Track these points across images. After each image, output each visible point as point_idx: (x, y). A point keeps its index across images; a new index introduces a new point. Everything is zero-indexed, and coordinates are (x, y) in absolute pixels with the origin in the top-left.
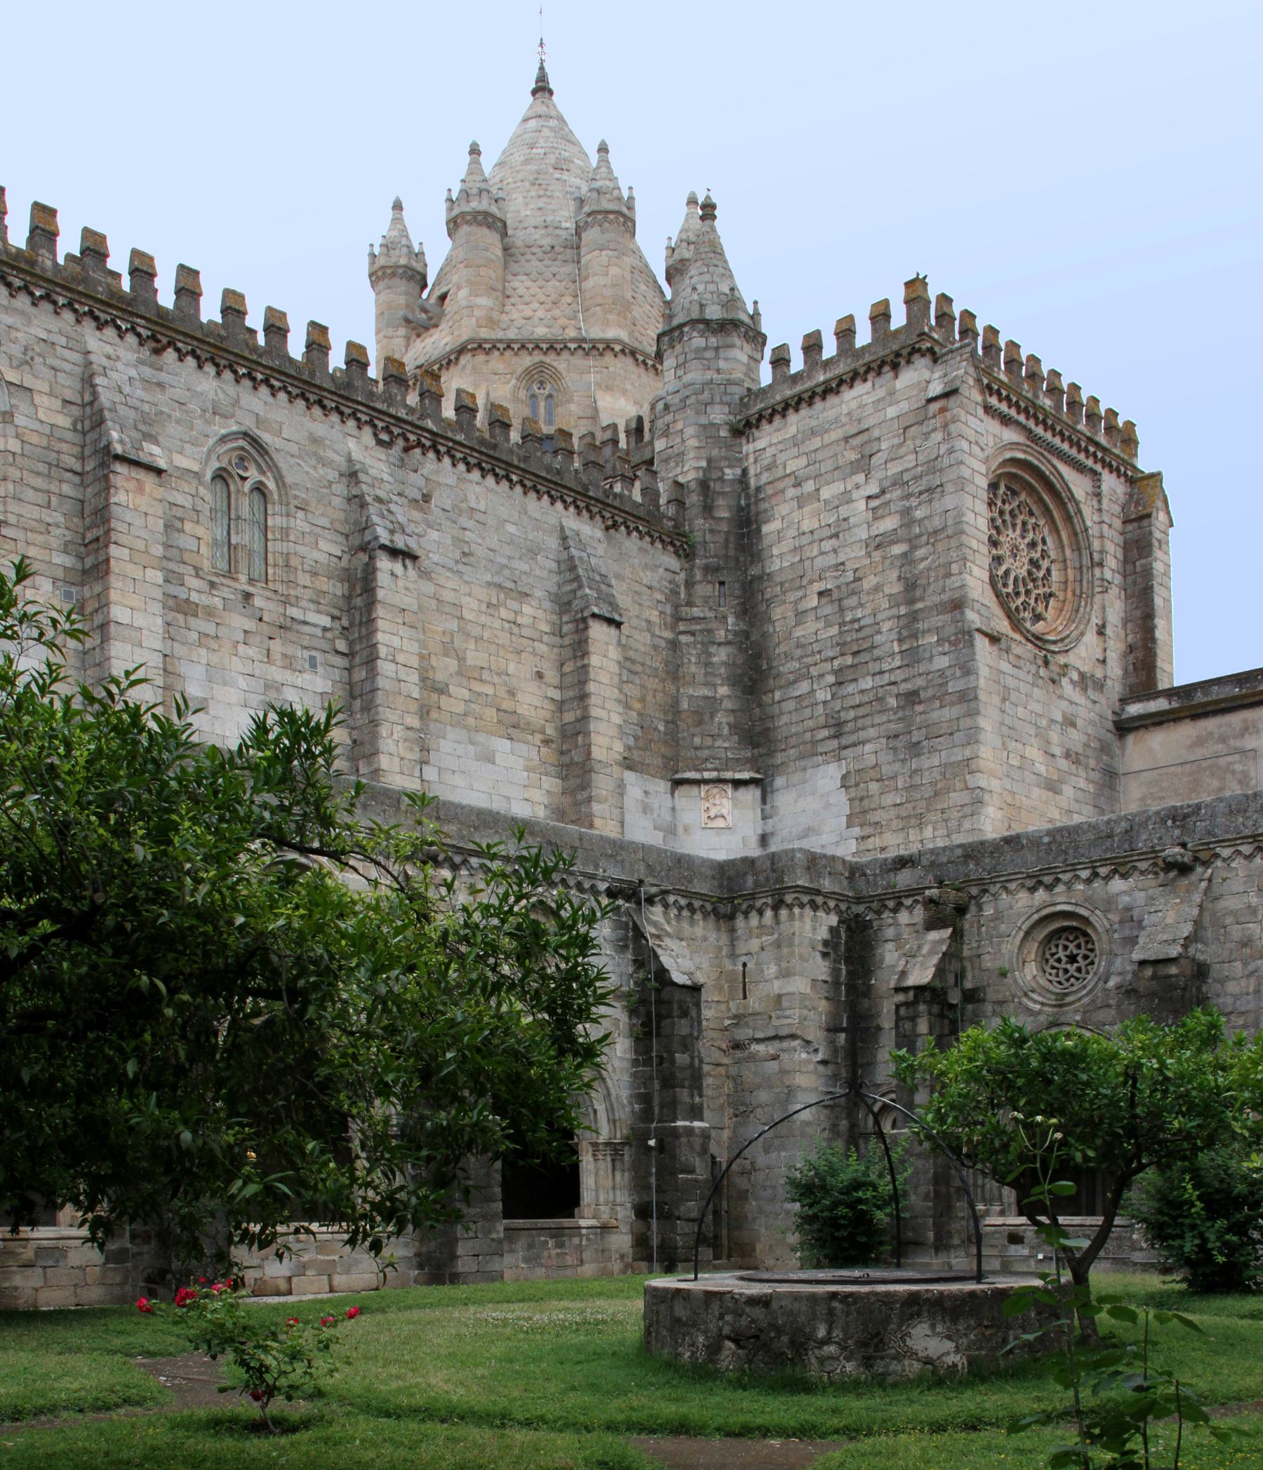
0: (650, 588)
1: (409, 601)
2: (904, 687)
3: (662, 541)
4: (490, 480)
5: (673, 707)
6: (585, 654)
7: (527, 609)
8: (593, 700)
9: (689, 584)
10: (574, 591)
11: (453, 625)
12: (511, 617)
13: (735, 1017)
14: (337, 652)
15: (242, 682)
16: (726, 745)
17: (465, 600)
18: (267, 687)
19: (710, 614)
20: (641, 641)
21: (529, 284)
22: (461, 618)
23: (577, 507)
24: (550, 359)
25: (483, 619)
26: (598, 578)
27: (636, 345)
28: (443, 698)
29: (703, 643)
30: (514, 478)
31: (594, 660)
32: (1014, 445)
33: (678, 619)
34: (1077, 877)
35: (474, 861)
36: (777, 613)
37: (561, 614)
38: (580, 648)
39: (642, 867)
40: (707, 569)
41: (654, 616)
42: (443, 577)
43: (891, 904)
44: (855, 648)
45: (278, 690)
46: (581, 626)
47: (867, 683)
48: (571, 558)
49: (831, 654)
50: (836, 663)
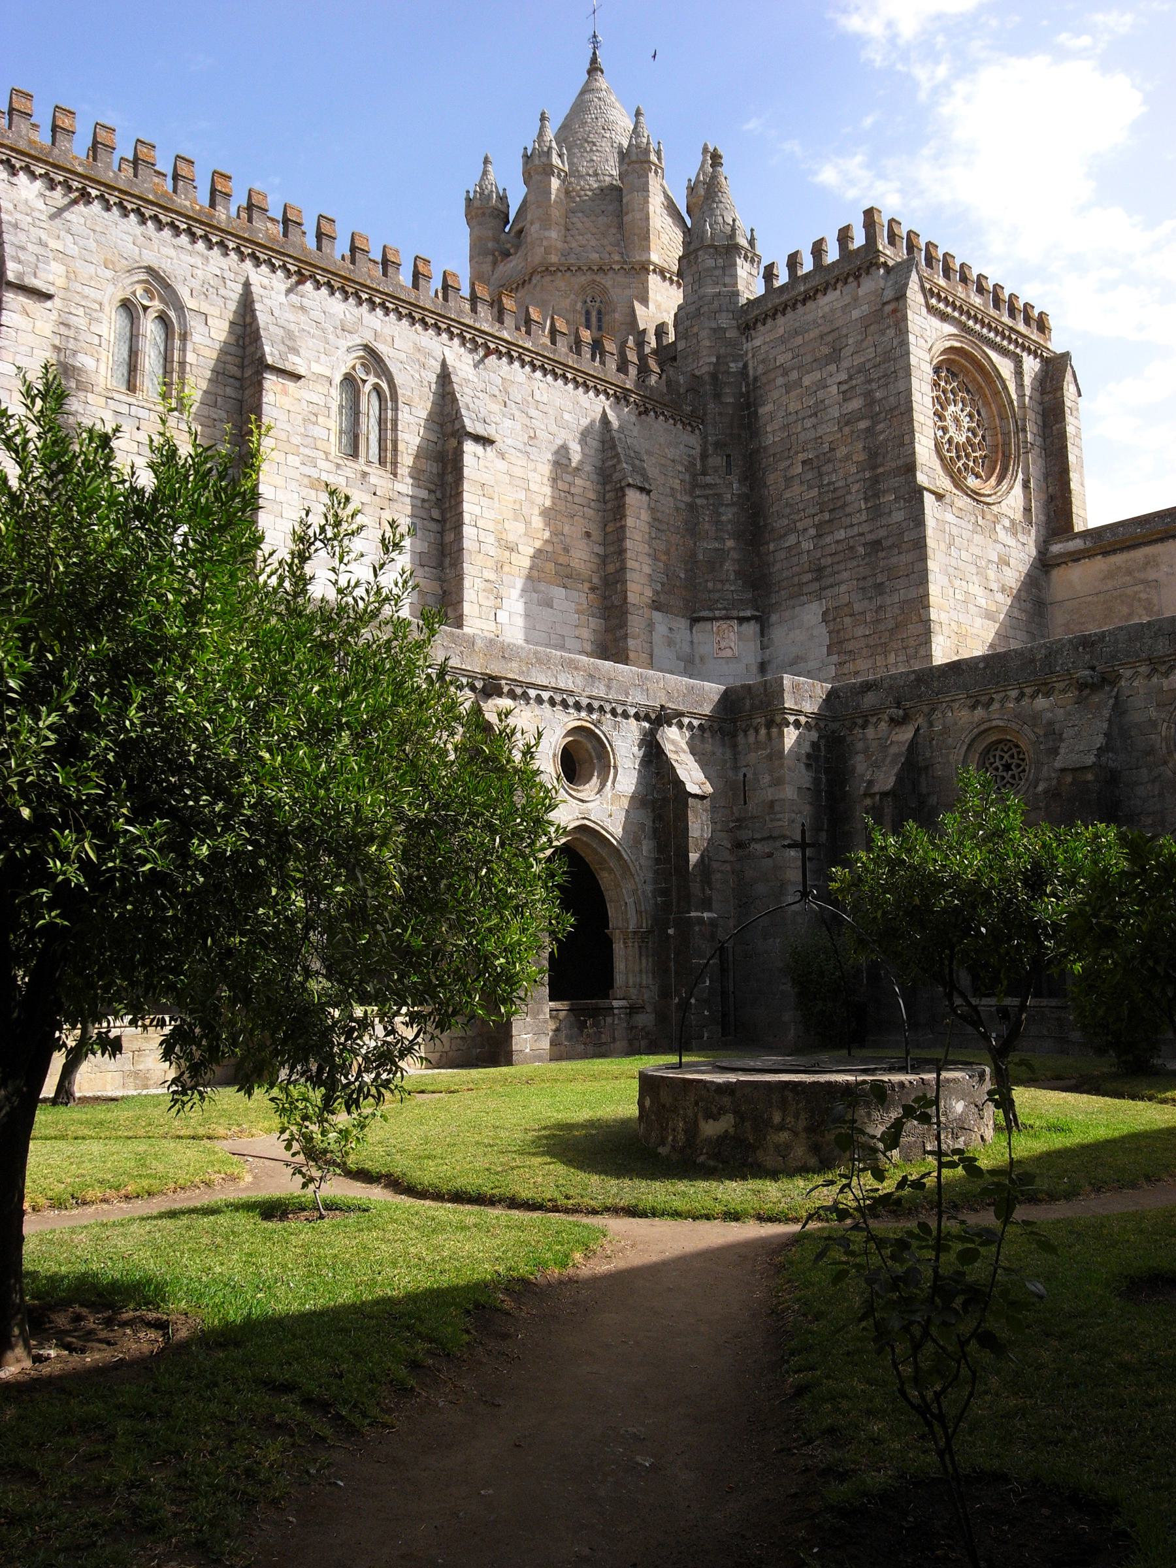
0: (673, 461)
1: (486, 478)
2: (870, 537)
3: (682, 422)
4: (549, 378)
8: (629, 554)
9: (704, 456)
11: (522, 495)
12: (566, 488)
14: (433, 519)
17: (531, 475)
20: (667, 505)
21: (585, 219)
26: (632, 454)
29: (713, 505)
31: (630, 522)
33: (694, 485)
35: (532, 693)
36: (771, 478)
37: (604, 484)
39: (662, 694)
40: (717, 445)
41: (676, 484)
42: (513, 455)
44: (831, 507)
46: (620, 494)
47: (841, 534)
49: (813, 512)
50: (817, 518)
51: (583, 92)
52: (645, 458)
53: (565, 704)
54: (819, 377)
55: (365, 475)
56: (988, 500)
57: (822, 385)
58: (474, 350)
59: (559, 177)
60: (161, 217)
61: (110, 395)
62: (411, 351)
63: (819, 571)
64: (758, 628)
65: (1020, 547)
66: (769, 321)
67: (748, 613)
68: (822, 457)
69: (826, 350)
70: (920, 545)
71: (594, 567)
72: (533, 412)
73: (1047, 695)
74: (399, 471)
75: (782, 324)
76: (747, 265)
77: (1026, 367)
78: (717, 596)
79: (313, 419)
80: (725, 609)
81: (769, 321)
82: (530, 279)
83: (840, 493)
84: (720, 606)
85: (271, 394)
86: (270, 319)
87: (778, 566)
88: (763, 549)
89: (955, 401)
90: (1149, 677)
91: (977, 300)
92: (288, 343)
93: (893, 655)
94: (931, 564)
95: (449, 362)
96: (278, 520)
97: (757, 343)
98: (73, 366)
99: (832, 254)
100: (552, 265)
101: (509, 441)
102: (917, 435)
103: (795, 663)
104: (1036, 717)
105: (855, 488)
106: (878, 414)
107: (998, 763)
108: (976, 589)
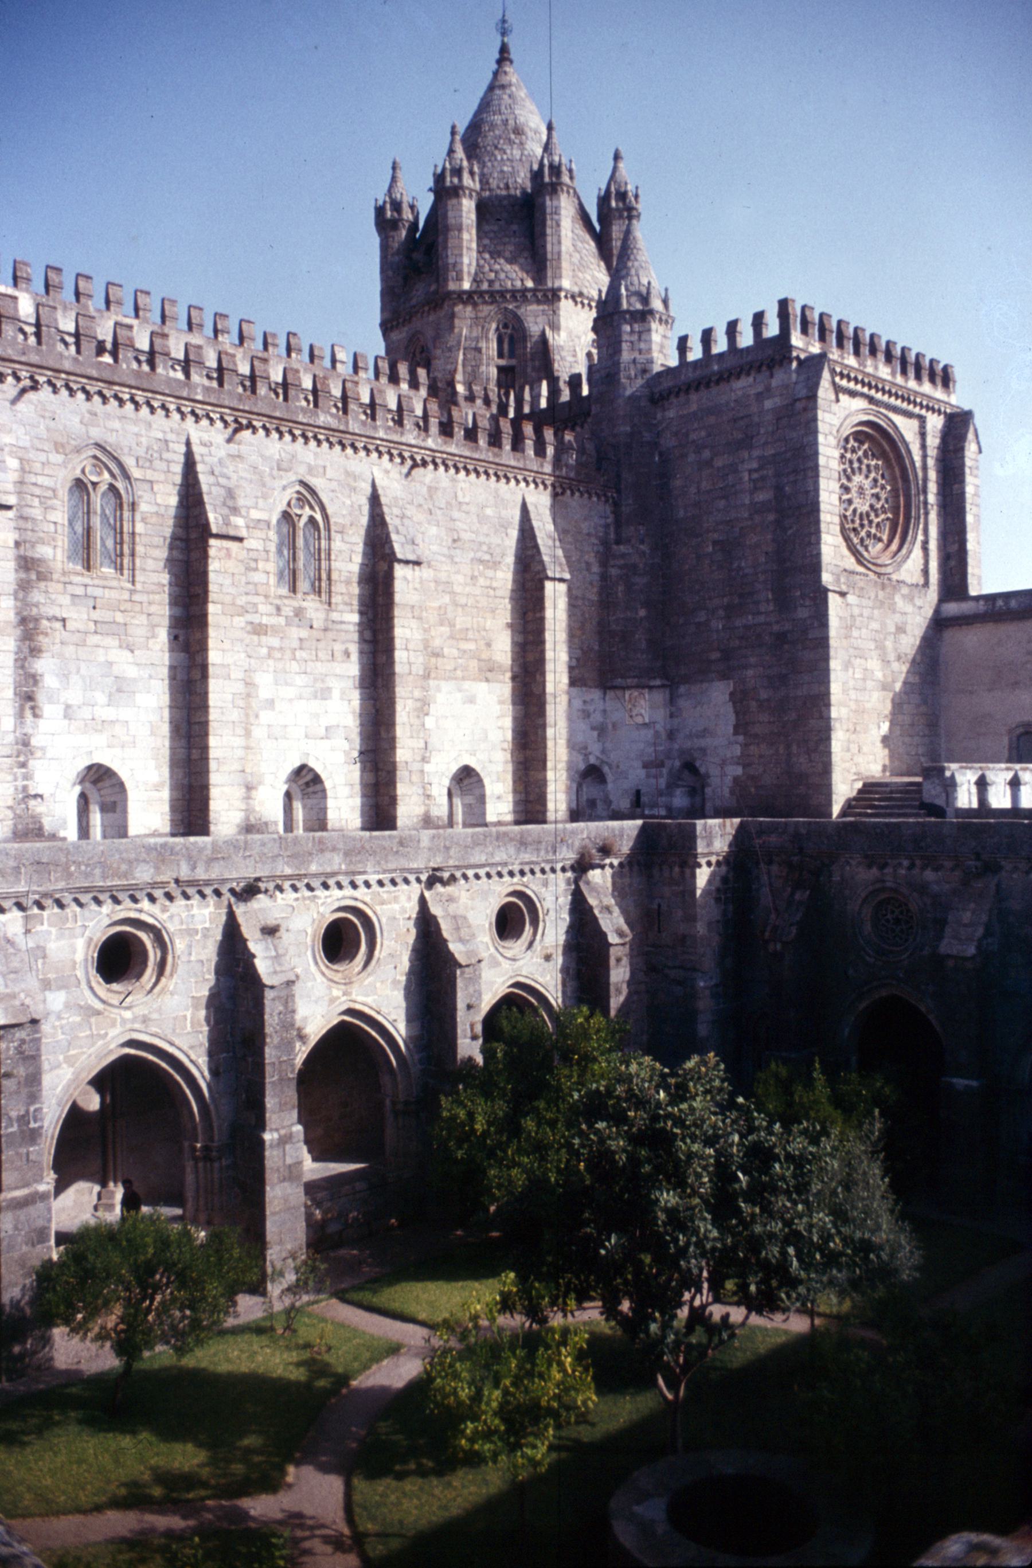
2: (776, 628)
9: (618, 524)
11: (447, 599)
12: (488, 583)
18: (316, 680)
22: (452, 593)
25: (468, 589)
28: (440, 660)
32: (864, 411)
45: (323, 681)
50: (726, 600)
51: (491, 88)
53: (500, 875)
56: (889, 570)
59: (471, 196)
61: (67, 580)
62: (342, 477)
63: (727, 655)
64: (668, 696)
66: (682, 398)
69: (738, 435)
72: (456, 514)
73: (936, 869)
74: (333, 600)
75: (695, 401)
76: (661, 329)
77: (929, 427)
79: (253, 565)
81: (682, 394)
86: (212, 479)
89: (860, 469)
92: (230, 503)
95: (377, 482)
96: (227, 682)
97: (671, 414)
98: (32, 559)
99: (746, 339)
104: (922, 888)
105: (761, 578)
107: (889, 916)
108: (874, 664)
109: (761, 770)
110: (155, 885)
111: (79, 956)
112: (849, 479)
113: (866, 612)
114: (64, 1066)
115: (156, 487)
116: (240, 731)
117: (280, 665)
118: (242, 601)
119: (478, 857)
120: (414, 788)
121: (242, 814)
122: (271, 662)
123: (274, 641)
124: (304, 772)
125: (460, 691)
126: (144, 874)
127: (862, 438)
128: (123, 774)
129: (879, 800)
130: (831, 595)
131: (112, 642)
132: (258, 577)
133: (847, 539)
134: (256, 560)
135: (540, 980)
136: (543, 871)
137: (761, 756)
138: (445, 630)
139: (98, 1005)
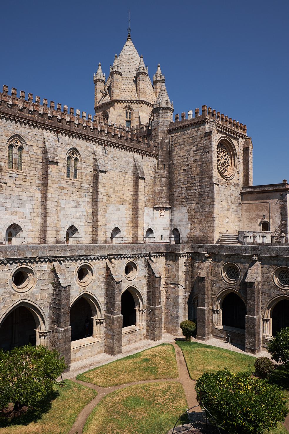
1: (104, 181)
5: (154, 192)
6: (138, 185)
7: (127, 176)
8: (139, 195)
9: (158, 164)
10: (136, 171)
11: (112, 182)
13: (167, 277)
14: (90, 192)
15: (72, 202)
16: (164, 200)
19: (162, 171)
23: (137, 152)
24: (130, 104)
25: (118, 179)
27: (147, 101)
29: (160, 177)
30: (125, 148)
31: (140, 187)
34: (235, 257)
35: (119, 257)
37: (133, 175)
38: (136, 184)
40: (162, 161)
41: (151, 173)
43: (198, 255)
45: (79, 202)
46: (137, 179)
47: (193, 191)
48: (135, 164)
52: (143, 167)
53: (127, 257)
54: (188, 148)
55: (73, 183)
57: (189, 150)
58: (102, 145)
60: (20, 120)
65: (236, 190)
67: (168, 206)
68: (189, 170)
69: (191, 141)
70: (212, 198)
71: (130, 198)
76: (171, 112)
78: (160, 201)
79: (60, 170)
80: (162, 205)
82: (112, 103)
83: (193, 180)
84: (161, 204)
85: (51, 168)
86: (50, 146)
87: (176, 195)
88: (173, 190)
90: (269, 260)
91: (229, 126)
92: (54, 153)
93: (205, 224)
94: (215, 203)
100: (118, 100)
101: (110, 168)
102: (213, 169)
103: (180, 222)
106: (203, 161)
107: (231, 271)
108: (225, 204)
109: (195, 230)
110: (32, 258)
111: (8, 278)
112: (219, 154)
113: (223, 189)
114: (3, 310)
115: (34, 148)
116: (55, 215)
117: (67, 198)
118: (57, 180)
119: (122, 252)
120: (103, 233)
121: (56, 239)
122: (64, 197)
123: (66, 191)
124: (73, 227)
125: (115, 207)
126: (29, 255)
127: (222, 143)
128: (22, 227)
129: (227, 240)
130: (215, 185)
131: (20, 190)
132: (62, 174)
133: (218, 170)
134: (61, 169)
135: (137, 286)
136: (138, 256)
137: (195, 227)
138: (112, 190)
139: (14, 292)
